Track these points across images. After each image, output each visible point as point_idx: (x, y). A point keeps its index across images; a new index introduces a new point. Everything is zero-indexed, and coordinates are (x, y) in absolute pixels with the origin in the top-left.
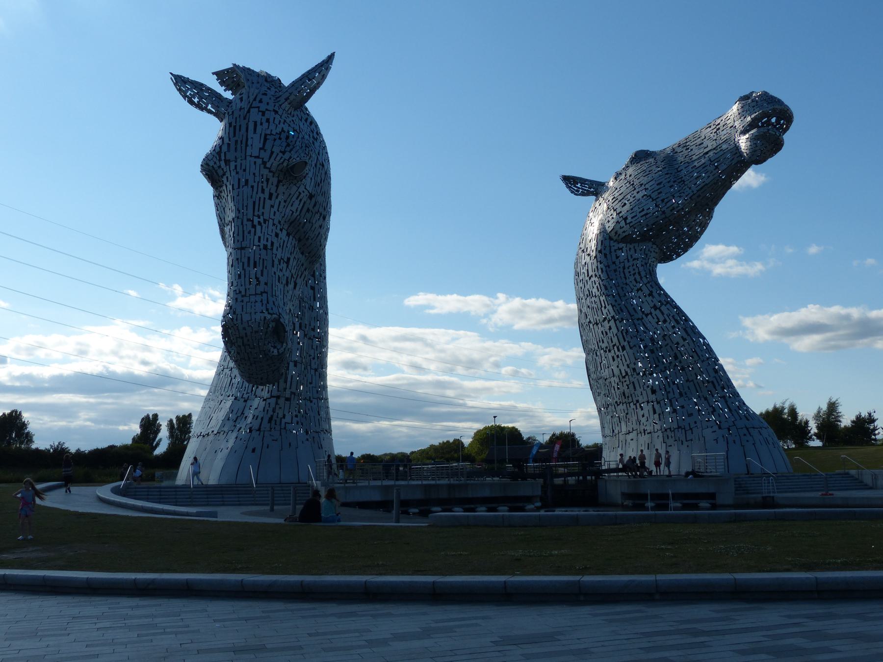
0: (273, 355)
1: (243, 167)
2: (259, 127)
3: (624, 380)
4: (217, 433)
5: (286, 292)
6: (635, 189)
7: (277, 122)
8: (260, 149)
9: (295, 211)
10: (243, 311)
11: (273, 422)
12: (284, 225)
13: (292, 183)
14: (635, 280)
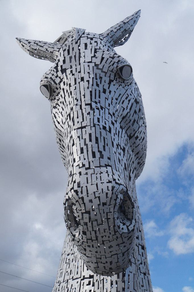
0: (123, 233)
1: (78, 70)
10: (87, 183)
13: (121, 85)
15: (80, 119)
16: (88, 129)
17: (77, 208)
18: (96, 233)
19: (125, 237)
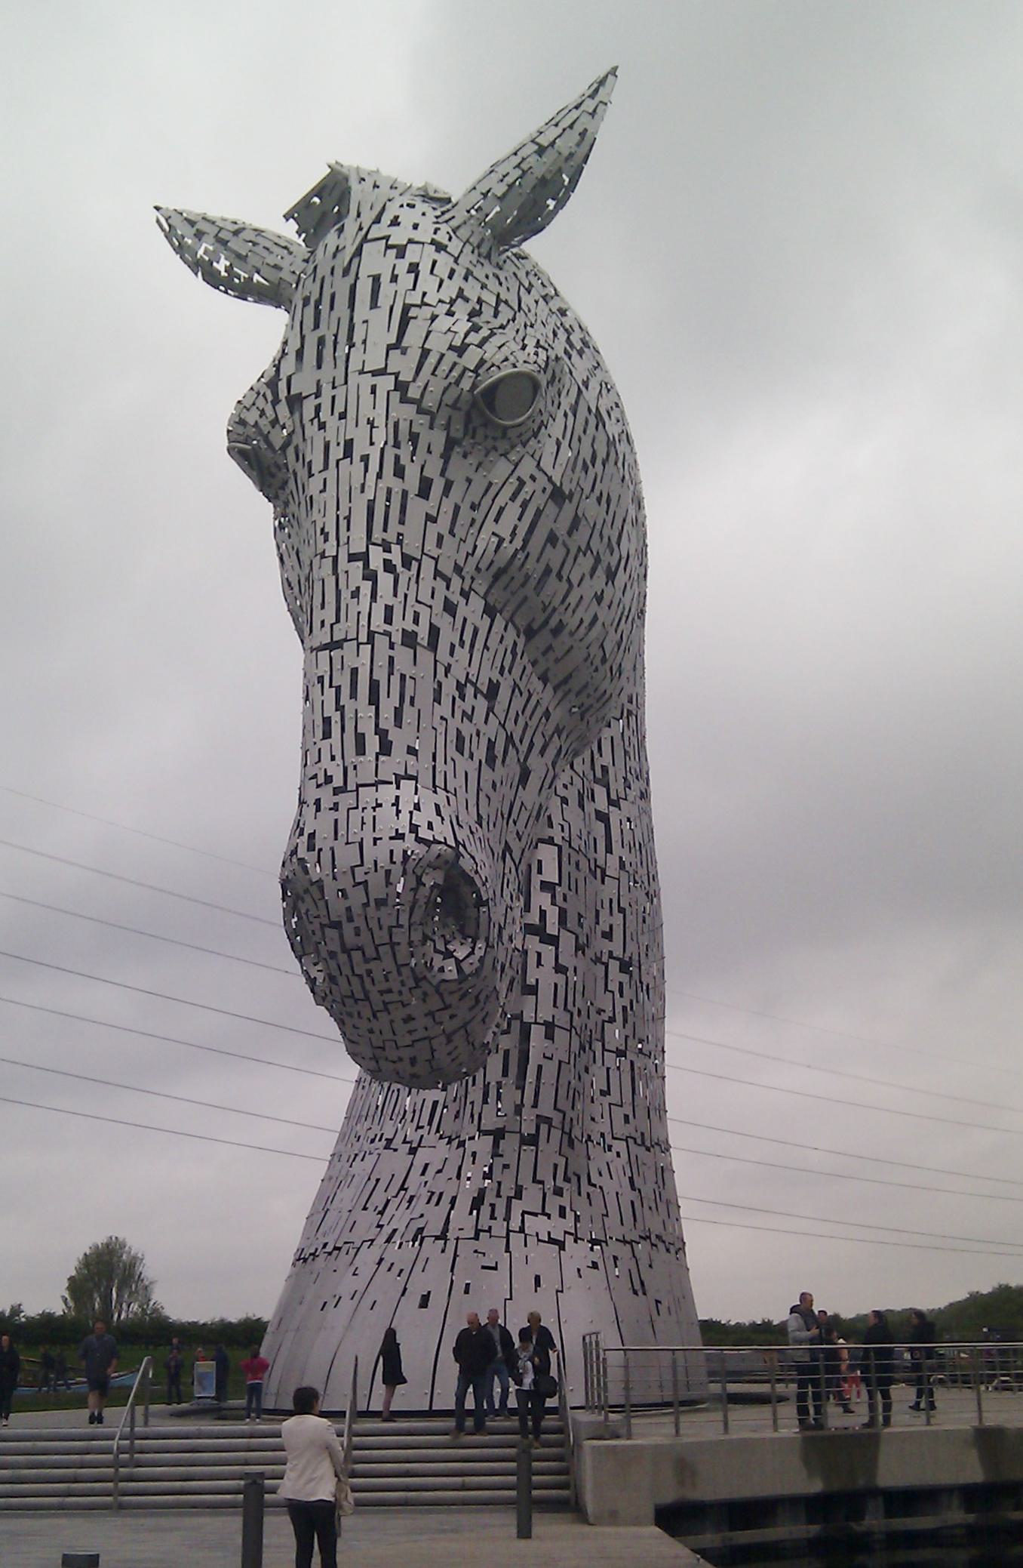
0: (444, 981)
1: (339, 408)
2: (386, 289)
5: (486, 786)
7: (442, 271)
8: (390, 348)
9: (506, 534)
10: (336, 839)
11: (485, 1210)
12: (473, 579)
15: (329, 615)
16: (350, 647)
17: (308, 910)
18: (362, 982)
19: (451, 993)
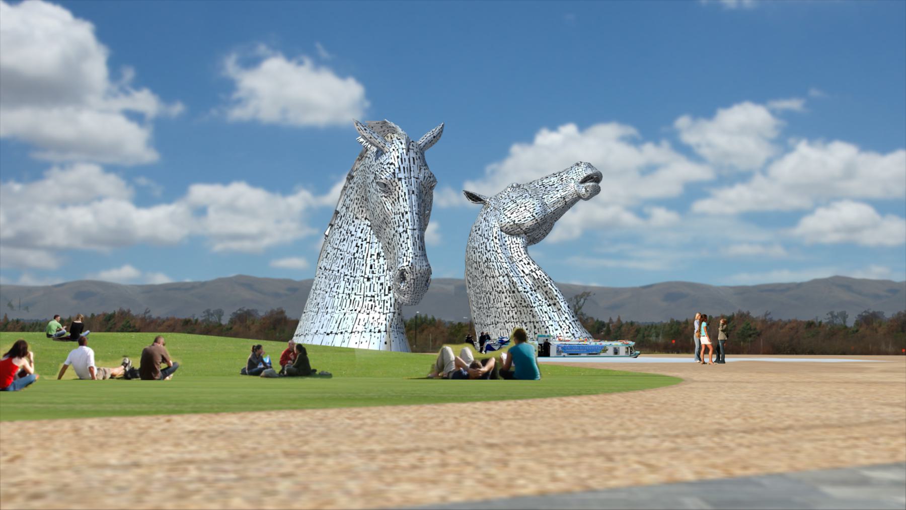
1: (410, 181)
3: (513, 309)
4: (352, 333)
6: (518, 205)
14: (518, 255)
